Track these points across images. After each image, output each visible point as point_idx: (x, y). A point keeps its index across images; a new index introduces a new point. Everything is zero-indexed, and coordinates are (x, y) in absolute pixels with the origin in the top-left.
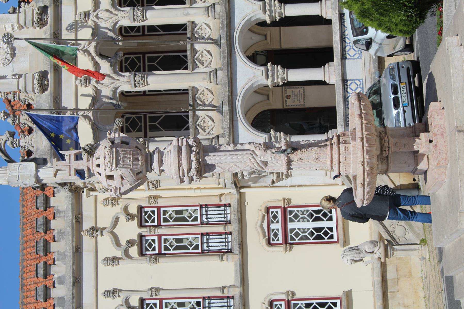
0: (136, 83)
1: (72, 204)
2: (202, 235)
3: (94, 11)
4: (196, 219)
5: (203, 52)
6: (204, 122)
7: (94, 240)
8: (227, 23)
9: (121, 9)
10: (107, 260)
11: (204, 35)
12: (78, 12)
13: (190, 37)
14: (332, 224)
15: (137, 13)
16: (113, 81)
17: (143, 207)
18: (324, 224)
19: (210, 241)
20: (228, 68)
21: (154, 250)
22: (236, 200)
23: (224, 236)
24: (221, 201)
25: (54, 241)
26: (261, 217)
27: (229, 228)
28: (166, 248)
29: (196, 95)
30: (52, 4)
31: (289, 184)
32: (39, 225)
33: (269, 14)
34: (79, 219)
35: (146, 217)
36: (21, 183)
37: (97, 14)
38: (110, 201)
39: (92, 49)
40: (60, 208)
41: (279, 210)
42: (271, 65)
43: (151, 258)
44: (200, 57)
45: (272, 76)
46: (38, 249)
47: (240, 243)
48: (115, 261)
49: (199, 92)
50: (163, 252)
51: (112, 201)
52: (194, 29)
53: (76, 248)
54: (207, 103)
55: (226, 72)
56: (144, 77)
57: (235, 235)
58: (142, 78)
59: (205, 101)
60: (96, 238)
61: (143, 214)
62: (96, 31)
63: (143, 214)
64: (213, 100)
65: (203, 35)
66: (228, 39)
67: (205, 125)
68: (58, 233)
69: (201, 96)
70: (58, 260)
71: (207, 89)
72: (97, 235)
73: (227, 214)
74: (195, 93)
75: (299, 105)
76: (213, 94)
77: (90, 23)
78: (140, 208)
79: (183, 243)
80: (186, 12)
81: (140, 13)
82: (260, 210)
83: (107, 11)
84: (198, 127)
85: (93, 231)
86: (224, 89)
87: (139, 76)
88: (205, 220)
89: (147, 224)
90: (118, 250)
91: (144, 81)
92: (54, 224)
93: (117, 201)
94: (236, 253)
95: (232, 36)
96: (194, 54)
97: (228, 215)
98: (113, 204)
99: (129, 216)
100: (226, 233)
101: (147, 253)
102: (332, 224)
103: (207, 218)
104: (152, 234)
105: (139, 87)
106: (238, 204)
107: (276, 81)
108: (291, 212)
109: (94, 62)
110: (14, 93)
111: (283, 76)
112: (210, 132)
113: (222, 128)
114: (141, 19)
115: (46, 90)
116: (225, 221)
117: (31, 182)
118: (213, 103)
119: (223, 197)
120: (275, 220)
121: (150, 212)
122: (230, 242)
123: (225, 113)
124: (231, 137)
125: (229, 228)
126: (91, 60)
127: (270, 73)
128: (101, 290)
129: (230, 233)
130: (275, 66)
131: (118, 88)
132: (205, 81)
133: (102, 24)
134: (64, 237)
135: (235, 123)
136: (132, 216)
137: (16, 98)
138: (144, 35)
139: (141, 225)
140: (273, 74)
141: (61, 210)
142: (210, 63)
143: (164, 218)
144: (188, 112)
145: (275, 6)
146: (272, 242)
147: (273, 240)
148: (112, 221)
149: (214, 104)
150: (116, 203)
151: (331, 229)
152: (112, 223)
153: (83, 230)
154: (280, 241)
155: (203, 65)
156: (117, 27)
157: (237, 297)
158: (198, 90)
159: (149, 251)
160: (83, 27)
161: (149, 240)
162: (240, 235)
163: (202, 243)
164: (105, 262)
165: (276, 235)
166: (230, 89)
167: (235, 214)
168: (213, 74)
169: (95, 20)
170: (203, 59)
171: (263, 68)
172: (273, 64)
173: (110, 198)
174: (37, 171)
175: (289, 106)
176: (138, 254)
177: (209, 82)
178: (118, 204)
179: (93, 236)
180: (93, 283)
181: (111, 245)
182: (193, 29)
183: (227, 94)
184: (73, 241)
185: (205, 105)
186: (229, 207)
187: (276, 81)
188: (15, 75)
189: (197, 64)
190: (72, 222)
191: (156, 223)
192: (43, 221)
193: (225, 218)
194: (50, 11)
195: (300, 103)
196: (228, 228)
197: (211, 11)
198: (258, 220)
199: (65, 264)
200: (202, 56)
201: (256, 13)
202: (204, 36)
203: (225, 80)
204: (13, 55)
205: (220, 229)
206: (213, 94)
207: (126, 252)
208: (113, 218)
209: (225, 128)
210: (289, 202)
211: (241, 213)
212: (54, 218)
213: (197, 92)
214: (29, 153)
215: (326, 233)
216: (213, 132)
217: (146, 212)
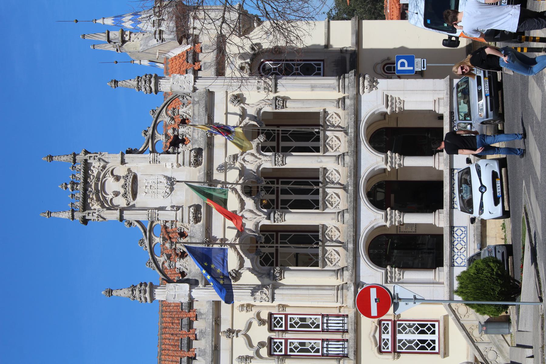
0: (275, 220)
1: (213, 309)
2: (323, 340)
3: (242, 155)
4: (318, 326)
5: (332, 195)
6: (331, 255)
7: (230, 340)
8: (354, 172)
9: (265, 153)
10: (241, 359)
11: (334, 180)
12: (228, 155)
13: (322, 182)
14: (435, 337)
15: (278, 159)
16: (256, 216)
17: (273, 314)
18: (428, 337)
19: (329, 346)
20: (353, 212)
21: (281, 351)
22: (353, 313)
23: (341, 343)
24: (340, 312)
25: (196, 339)
26: (374, 328)
27: (346, 336)
28: (291, 350)
29: (325, 231)
30: (207, 148)
32: (184, 325)
33: (390, 165)
34: (218, 322)
35: (275, 322)
36: (177, 300)
37: (244, 158)
38: (245, 308)
39: (238, 188)
40: (202, 311)
41: (390, 323)
42: (390, 210)
43: (278, 358)
44: (330, 199)
45: (391, 219)
46: (182, 345)
47: (355, 350)
48: (247, 359)
49: (328, 229)
50: (289, 353)
51: (247, 308)
52: (326, 174)
53: (215, 347)
54: (334, 239)
55: (352, 215)
56: (282, 215)
57: (352, 343)
58: (281, 215)
59: (333, 237)
60: (232, 339)
61: (273, 320)
62: (243, 172)
63: (273, 320)
64: (339, 237)
65: (333, 179)
66: (355, 186)
67: (332, 257)
68: (200, 332)
69: (330, 233)
70: (199, 356)
71: (335, 227)
72: (233, 336)
73: (345, 324)
74: (325, 230)
75: (411, 232)
76: (339, 232)
77: (237, 165)
79: (305, 346)
80: (319, 160)
81: (281, 159)
82: (374, 322)
83: (253, 155)
84: (326, 259)
85: (230, 332)
86: (350, 229)
87: (278, 214)
88: (325, 327)
89: (276, 329)
90: (250, 350)
91: (282, 218)
92: (196, 324)
93: (251, 308)
94: (351, 358)
95: (358, 183)
96: (325, 196)
97: (346, 324)
98: (247, 310)
99: (260, 322)
100: (343, 340)
101: (275, 353)
102: (435, 337)
103: (327, 326)
105: (278, 222)
106: (355, 316)
107: (393, 224)
108: (400, 325)
109: (240, 199)
110: (172, 222)
111: (400, 220)
112: (336, 264)
113: (347, 262)
114: (281, 164)
115: (200, 221)
116: (343, 330)
117: (186, 300)
118: (340, 239)
119: (342, 309)
120: (386, 331)
121: (278, 318)
122: (346, 348)
123: (349, 250)
124: (354, 271)
125: (346, 336)
126: (237, 197)
127: (389, 217)
129: (347, 340)
130: (394, 211)
131: (260, 222)
132: (334, 220)
133: (248, 167)
134: (205, 336)
135: (357, 258)
136: (264, 322)
137: (174, 227)
139: (271, 330)
140: (391, 218)
141: (202, 313)
142: (338, 205)
143: (290, 324)
144: (318, 248)
145: (395, 158)
146: (383, 350)
147: (384, 348)
148: (246, 325)
149: (340, 240)
150: (250, 309)
151: (434, 341)
152: (246, 327)
153: (221, 331)
154: (390, 350)
155: (332, 206)
156: (260, 169)
158: (327, 228)
159: (277, 352)
160: (231, 168)
161: (277, 342)
162: (356, 343)
163: (323, 348)
164: (239, 360)
165: (386, 344)
166: (354, 230)
167: (351, 325)
168: (341, 216)
169: (242, 162)
170: (332, 200)
171: (383, 213)
172: (392, 209)
173: (245, 305)
174: (190, 291)
175: (402, 232)
176: (268, 355)
177: (337, 221)
178: (251, 310)
179: (230, 337)
181: (245, 345)
182: (324, 174)
183: (352, 234)
184: (212, 341)
185: (332, 241)
186: (346, 317)
187: (393, 224)
188: (173, 207)
189: (327, 205)
190: (212, 324)
191: (283, 328)
192: (187, 322)
193: (343, 327)
194: (204, 154)
195: (412, 230)
196: (345, 336)
197: (341, 161)
198: (371, 330)
199: (205, 360)
200: (332, 198)
201: (379, 164)
202: (334, 180)
203: (351, 222)
204: (172, 189)
205: (338, 336)
206: (339, 232)
207: (257, 353)
208: (247, 322)
209: (349, 263)
210: (399, 316)
211: (357, 324)
212: (196, 320)
213: (327, 229)
214: (183, 274)
215: (429, 345)
216: (338, 264)
217: (275, 318)
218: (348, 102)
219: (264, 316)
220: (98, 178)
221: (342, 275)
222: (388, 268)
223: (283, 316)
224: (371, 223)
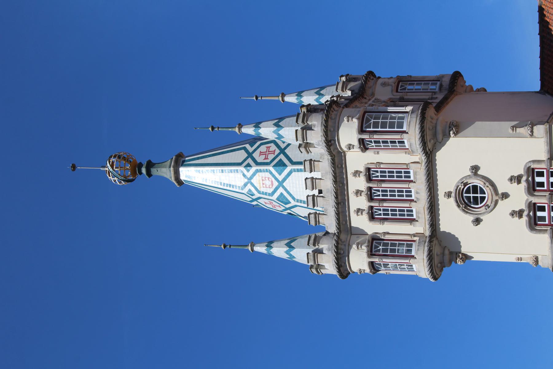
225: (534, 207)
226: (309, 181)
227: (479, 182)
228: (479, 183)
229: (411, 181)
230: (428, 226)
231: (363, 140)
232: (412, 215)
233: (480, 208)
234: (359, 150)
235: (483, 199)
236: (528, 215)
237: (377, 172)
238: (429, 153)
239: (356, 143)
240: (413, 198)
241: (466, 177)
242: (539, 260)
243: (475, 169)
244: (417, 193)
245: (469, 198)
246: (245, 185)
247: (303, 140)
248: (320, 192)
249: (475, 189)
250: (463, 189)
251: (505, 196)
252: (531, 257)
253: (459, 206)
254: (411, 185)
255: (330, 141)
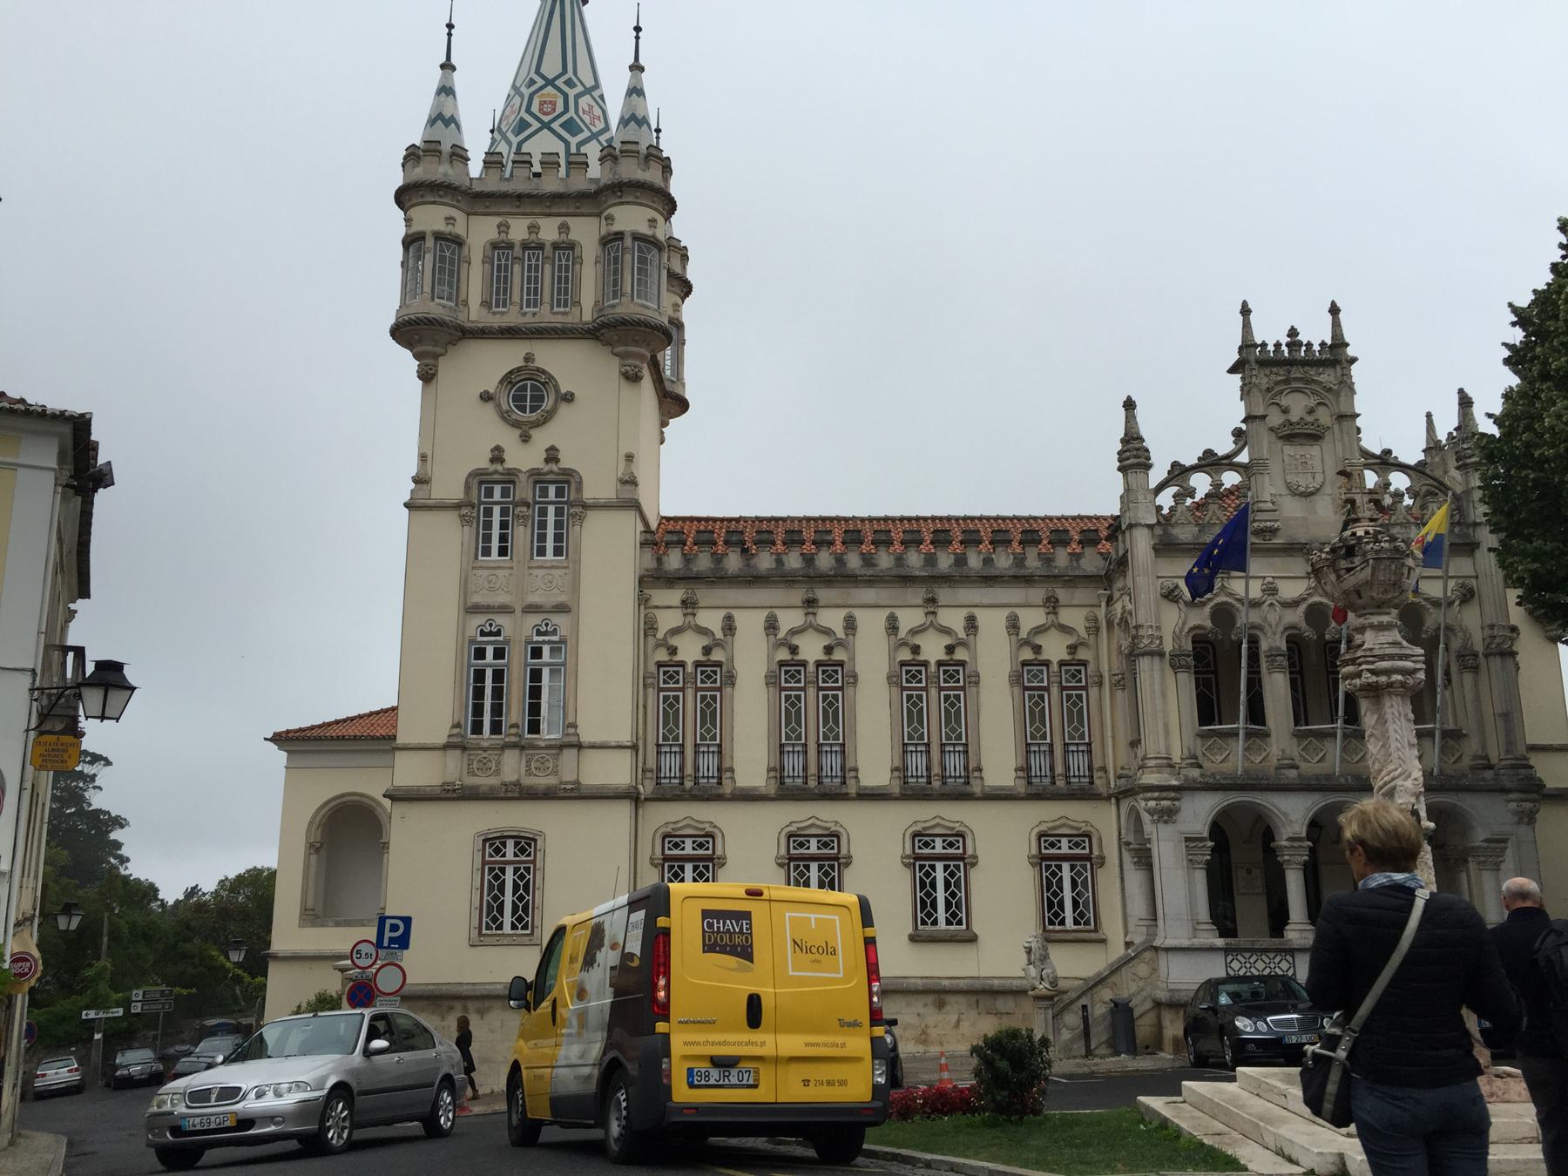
31: (1125, 867)
78: (1084, 663)
104: (1051, 679)
128: (976, 611)
138: (1328, 673)
157: (968, 788)
180: (985, 602)
218: (1489, 774)
219: (1082, 654)
220: (1309, 381)
221: (1192, 765)
222: (1210, 844)
223: (1083, 684)
224: (1285, 814)
225: (510, 478)
226: (554, 159)
227: (551, 402)
228: (548, 404)
229: (552, 308)
230: (481, 325)
231: (622, 239)
232: (497, 306)
233: (506, 402)
234: (603, 232)
235: (522, 409)
236: (496, 472)
237: (568, 260)
238: (598, 334)
239: (616, 228)
240: (525, 309)
241: (556, 387)
242: (425, 486)
243: (569, 398)
244: (534, 314)
245: (524, 388)
246: (543, 77)
247: (621, 152)
248: (537, 175)
249: (536, 399)
250: (539, 382)
251: (526, 439)
252: (427, 474)
253: (511, 372)
254: (547, 307)
255: (620, 191)
